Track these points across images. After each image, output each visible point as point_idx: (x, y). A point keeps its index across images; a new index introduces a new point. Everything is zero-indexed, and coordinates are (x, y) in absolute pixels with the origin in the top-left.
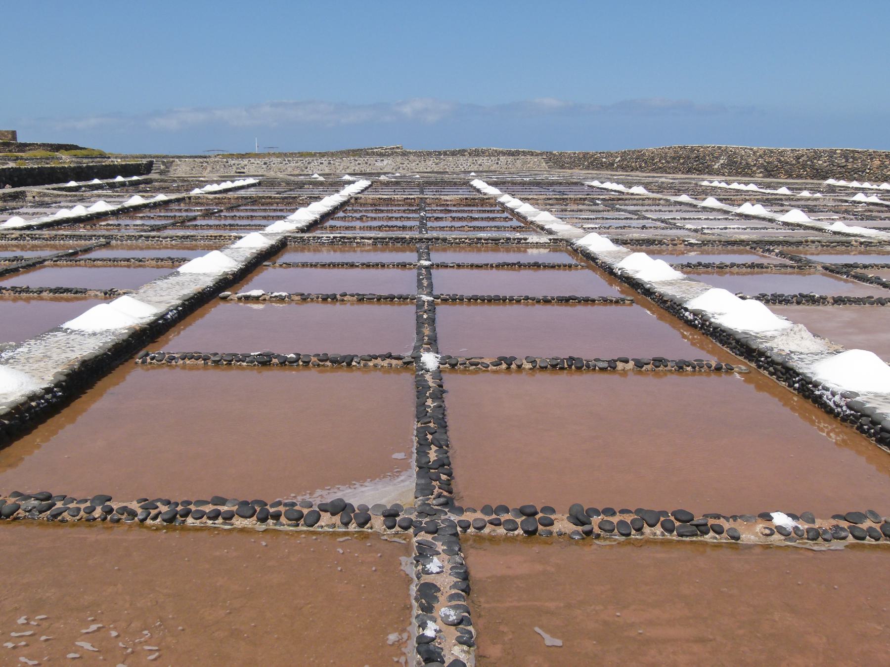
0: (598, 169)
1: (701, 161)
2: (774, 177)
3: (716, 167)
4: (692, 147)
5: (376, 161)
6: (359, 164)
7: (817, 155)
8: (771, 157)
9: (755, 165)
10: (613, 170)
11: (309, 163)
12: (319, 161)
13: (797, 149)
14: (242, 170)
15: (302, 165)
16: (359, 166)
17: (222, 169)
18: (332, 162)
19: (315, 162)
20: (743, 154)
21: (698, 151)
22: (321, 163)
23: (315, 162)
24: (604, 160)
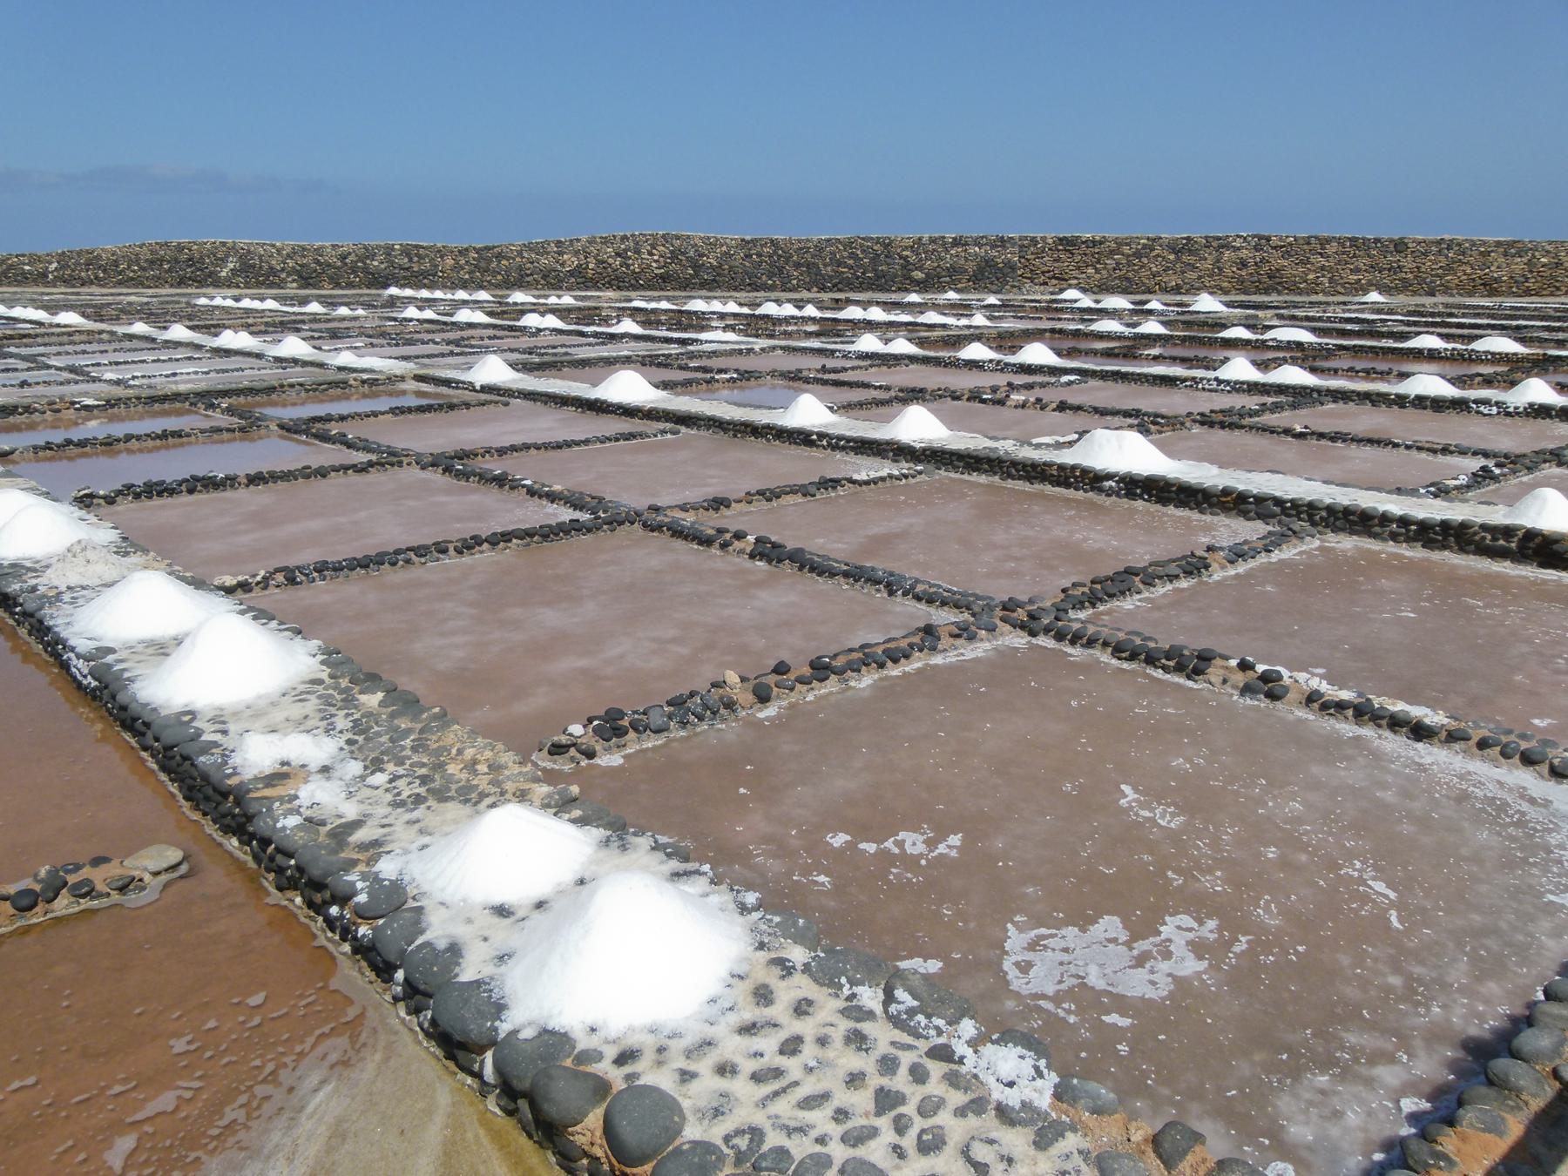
0: (19, 284)
1: (198, 265)
2: (314, 286)
3: (223, 274)
4: (179, 244)
7: (369, 253)
8: (304, 256)
9: (283, 270)
10: (47, 284)
13: (340, 244)
20: (262, 253)
21: (190, 250)
24: (27, 268)
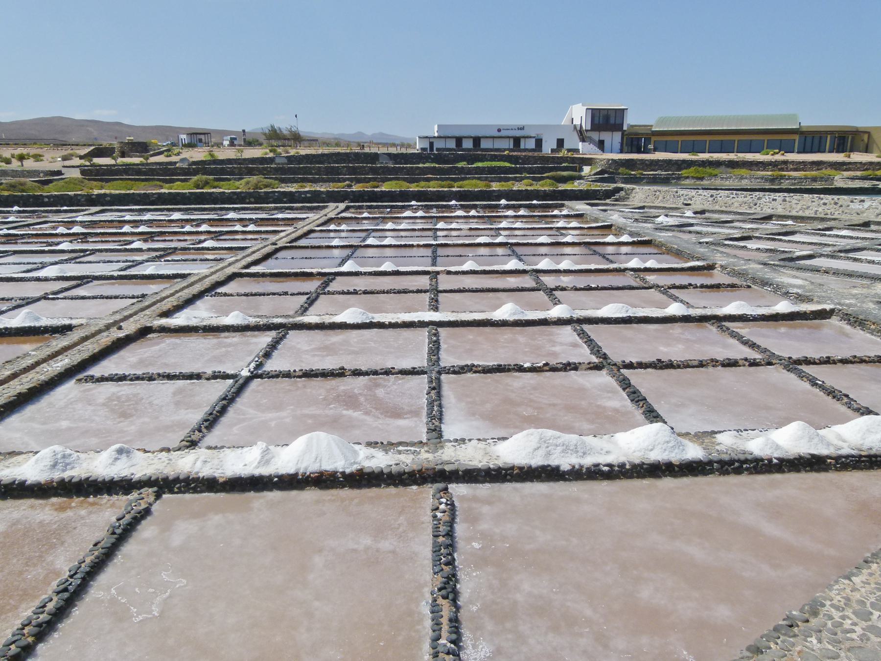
5: (852, 202)
6: (825, 204)
11: (759, 199)
12: (772, 197)
14: (689, 202)
15: (751, 200)
16: (824, 207)
17: (671, 200)
18: (787, 199)
19: (767, 197)
22: (774, 200)
23: (767, 197)
